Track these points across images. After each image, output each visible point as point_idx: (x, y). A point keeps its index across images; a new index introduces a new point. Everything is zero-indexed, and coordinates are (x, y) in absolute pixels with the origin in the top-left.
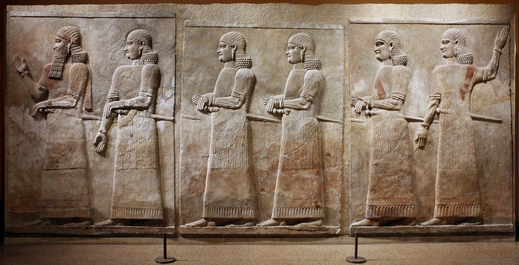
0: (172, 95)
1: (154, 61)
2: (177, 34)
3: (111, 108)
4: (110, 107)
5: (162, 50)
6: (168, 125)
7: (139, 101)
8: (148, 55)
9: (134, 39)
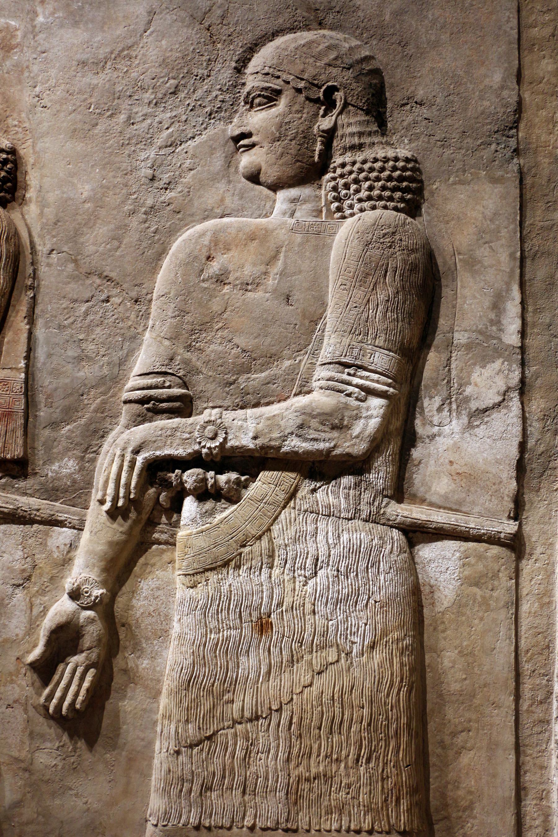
0: (508, 389)
1: (398, 195)
2: (527, 60)
3: (140, 459)
4: (136, 452)
5: (444, 140)
6: (480, 567)
7: (314, 423)
8: (364, 162)
9: (284, 76)
